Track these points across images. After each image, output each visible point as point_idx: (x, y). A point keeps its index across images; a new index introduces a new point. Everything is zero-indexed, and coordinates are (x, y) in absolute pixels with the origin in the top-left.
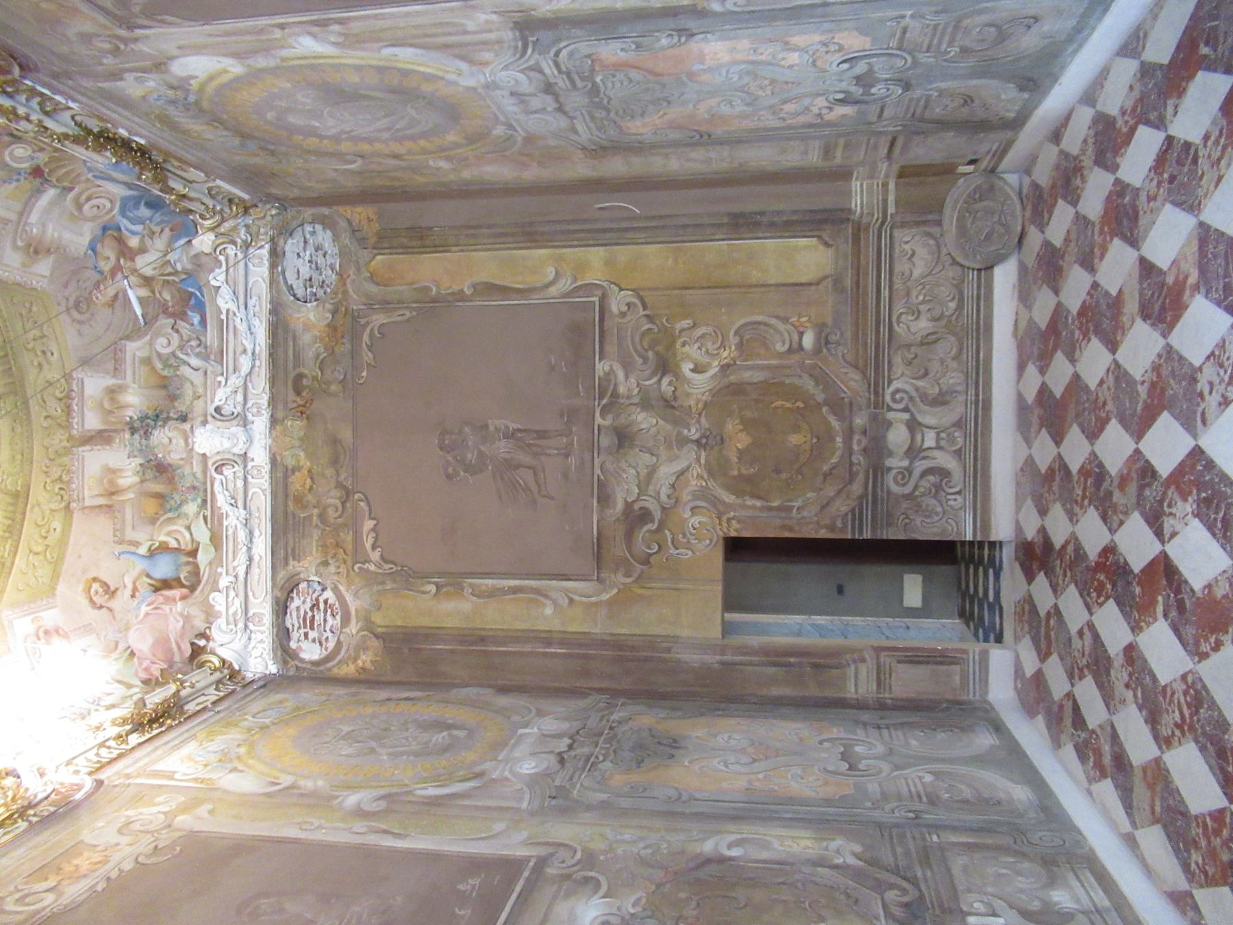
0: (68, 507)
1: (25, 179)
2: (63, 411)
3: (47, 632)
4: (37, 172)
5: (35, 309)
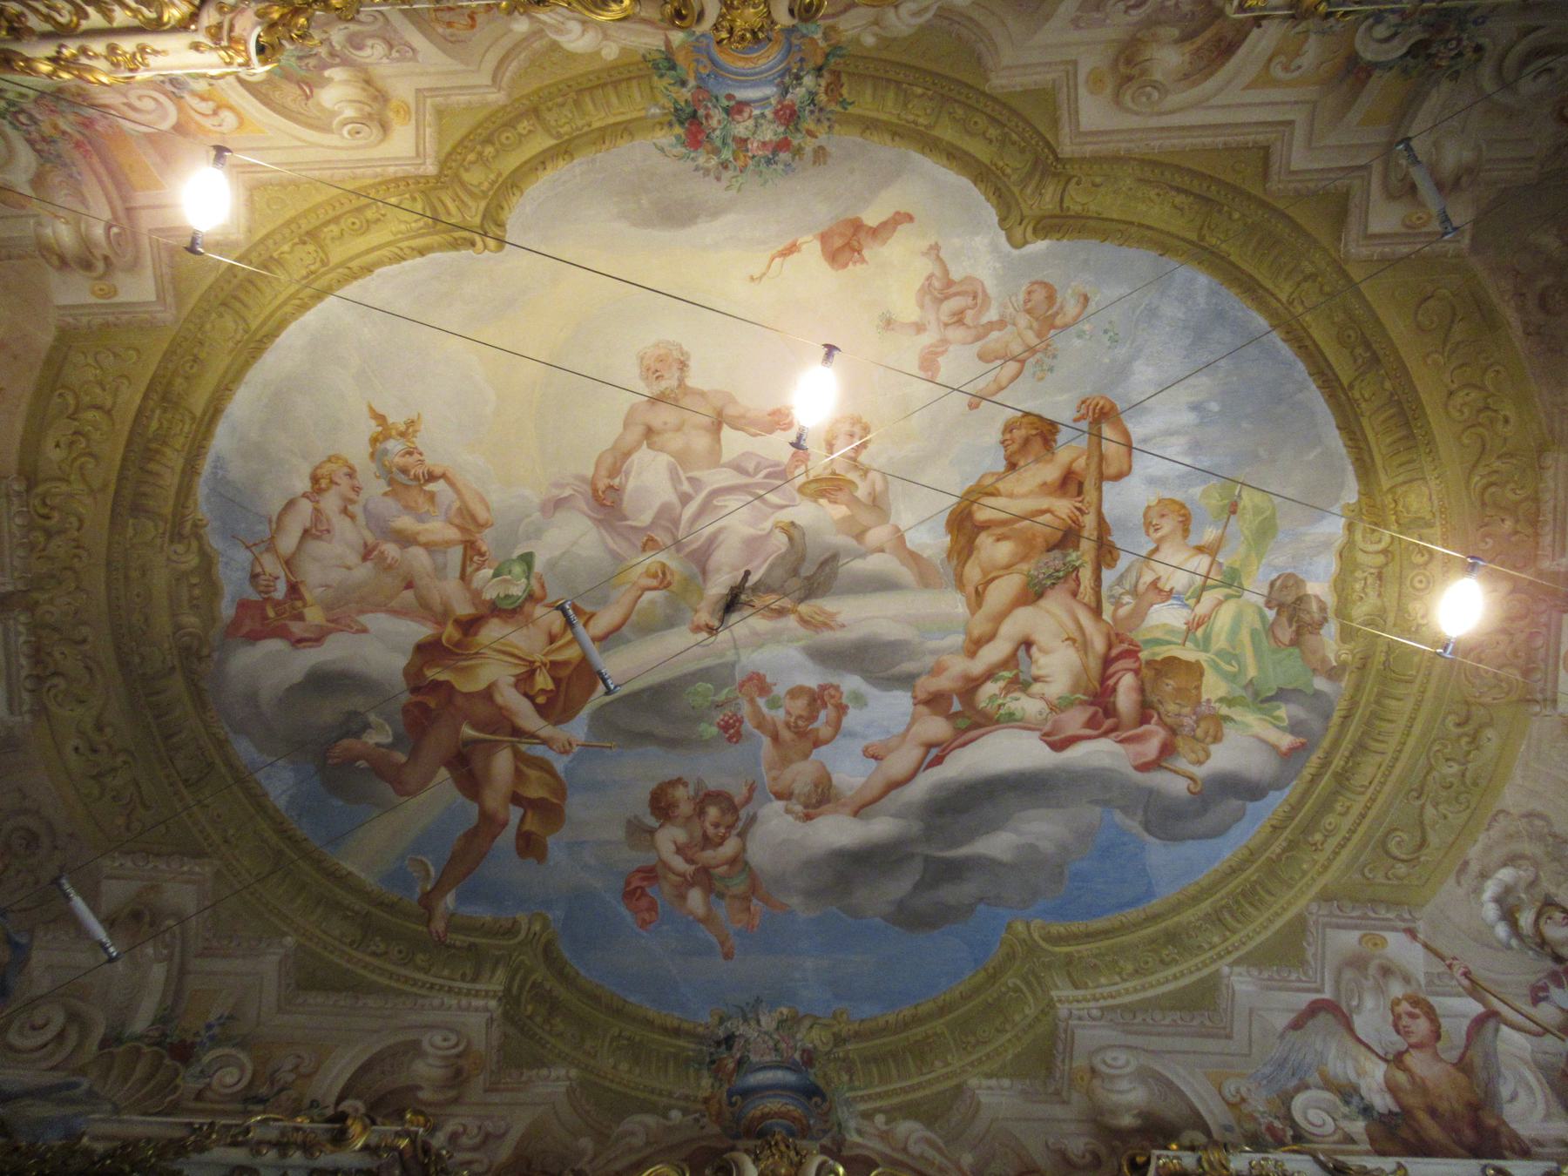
0: (30, 487)
1: (197, 1034)
2: (49, 654)
3: (87, 265)
4: (184, 1053)
5: (120, 821)
